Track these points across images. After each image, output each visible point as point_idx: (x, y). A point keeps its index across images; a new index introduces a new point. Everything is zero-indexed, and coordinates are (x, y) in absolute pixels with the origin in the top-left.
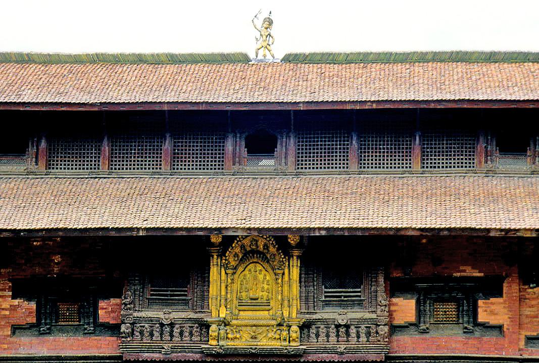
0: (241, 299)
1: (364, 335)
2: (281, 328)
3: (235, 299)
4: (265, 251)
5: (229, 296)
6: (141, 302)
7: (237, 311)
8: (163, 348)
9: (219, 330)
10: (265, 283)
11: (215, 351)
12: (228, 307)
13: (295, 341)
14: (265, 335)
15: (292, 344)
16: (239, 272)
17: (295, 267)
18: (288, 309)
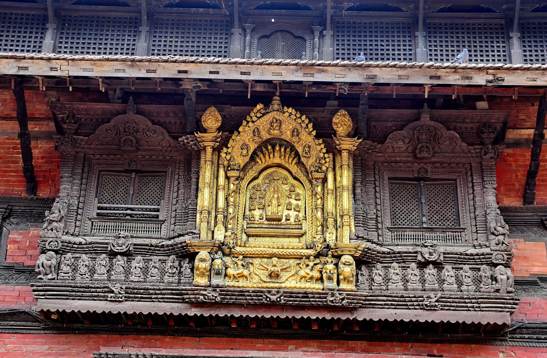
0: (251, 219)
1: (469, 280)
2: (323, 259)
3: (241, 218)
4: (295, 139)
5: (231, 210)
6: (78, 223)
7: (244, 237)
8: (112, 292)
9: (213, 260)
10: (293, 197)
11: (204, 295)
12: (230, 226)
13: (349, 282)
14: (293, 272)
15: (343, 286)
16: (249, 177)
17: (345, 167)
18: (335, 232)
